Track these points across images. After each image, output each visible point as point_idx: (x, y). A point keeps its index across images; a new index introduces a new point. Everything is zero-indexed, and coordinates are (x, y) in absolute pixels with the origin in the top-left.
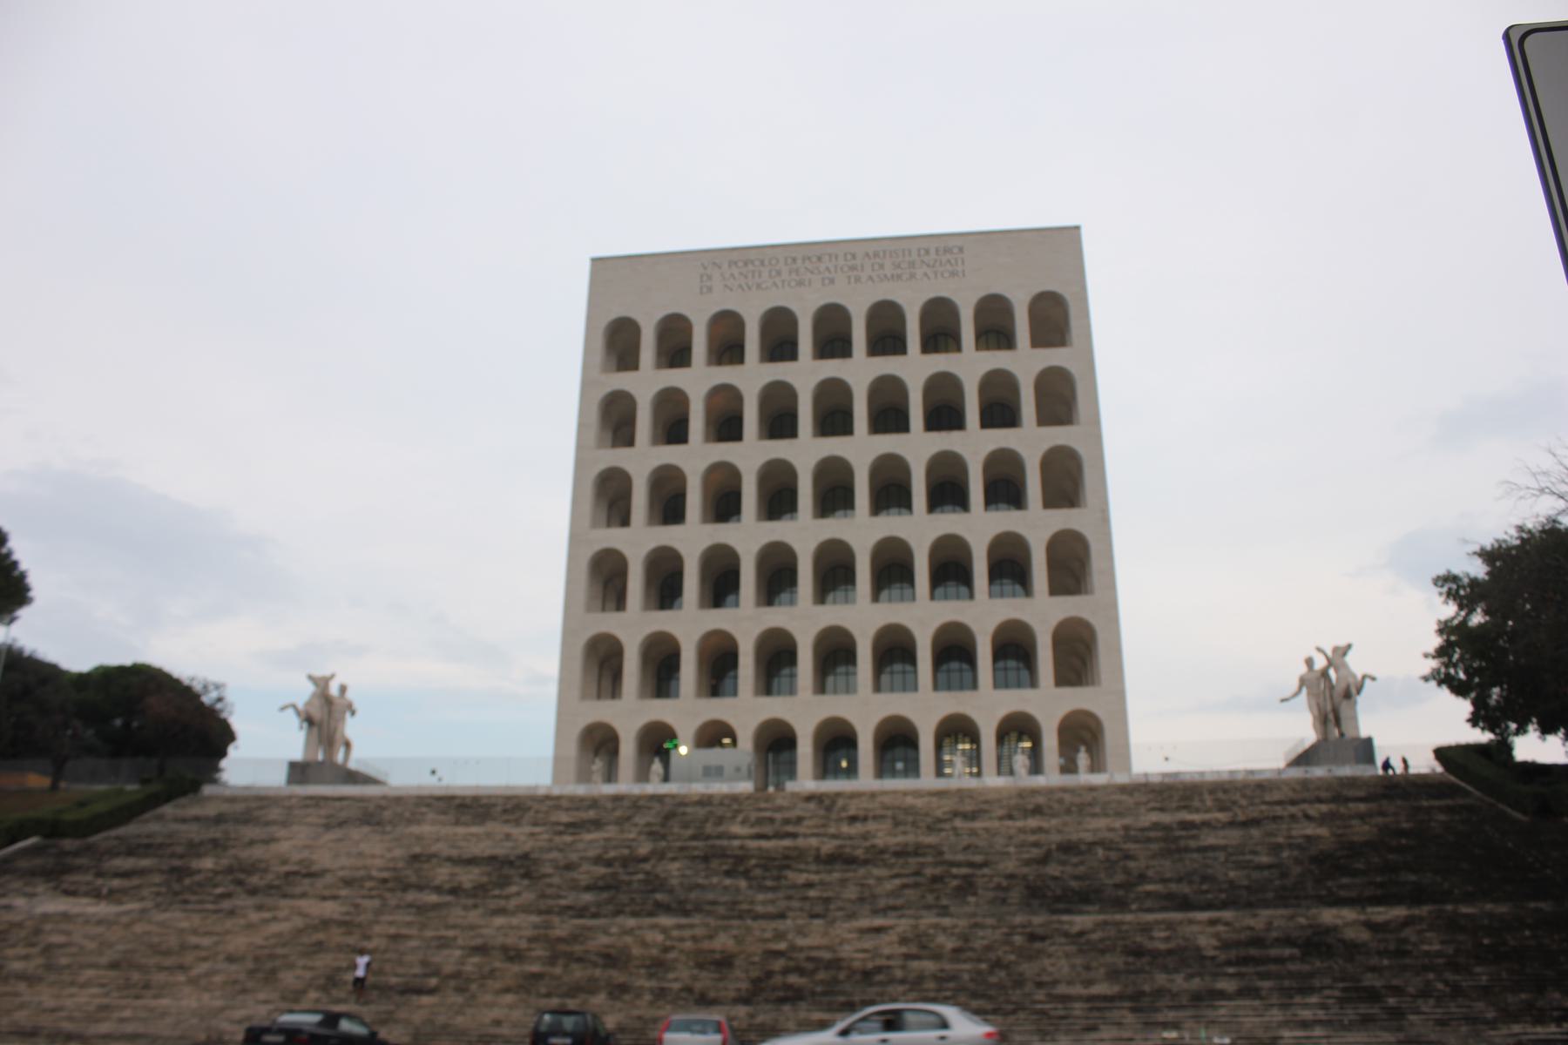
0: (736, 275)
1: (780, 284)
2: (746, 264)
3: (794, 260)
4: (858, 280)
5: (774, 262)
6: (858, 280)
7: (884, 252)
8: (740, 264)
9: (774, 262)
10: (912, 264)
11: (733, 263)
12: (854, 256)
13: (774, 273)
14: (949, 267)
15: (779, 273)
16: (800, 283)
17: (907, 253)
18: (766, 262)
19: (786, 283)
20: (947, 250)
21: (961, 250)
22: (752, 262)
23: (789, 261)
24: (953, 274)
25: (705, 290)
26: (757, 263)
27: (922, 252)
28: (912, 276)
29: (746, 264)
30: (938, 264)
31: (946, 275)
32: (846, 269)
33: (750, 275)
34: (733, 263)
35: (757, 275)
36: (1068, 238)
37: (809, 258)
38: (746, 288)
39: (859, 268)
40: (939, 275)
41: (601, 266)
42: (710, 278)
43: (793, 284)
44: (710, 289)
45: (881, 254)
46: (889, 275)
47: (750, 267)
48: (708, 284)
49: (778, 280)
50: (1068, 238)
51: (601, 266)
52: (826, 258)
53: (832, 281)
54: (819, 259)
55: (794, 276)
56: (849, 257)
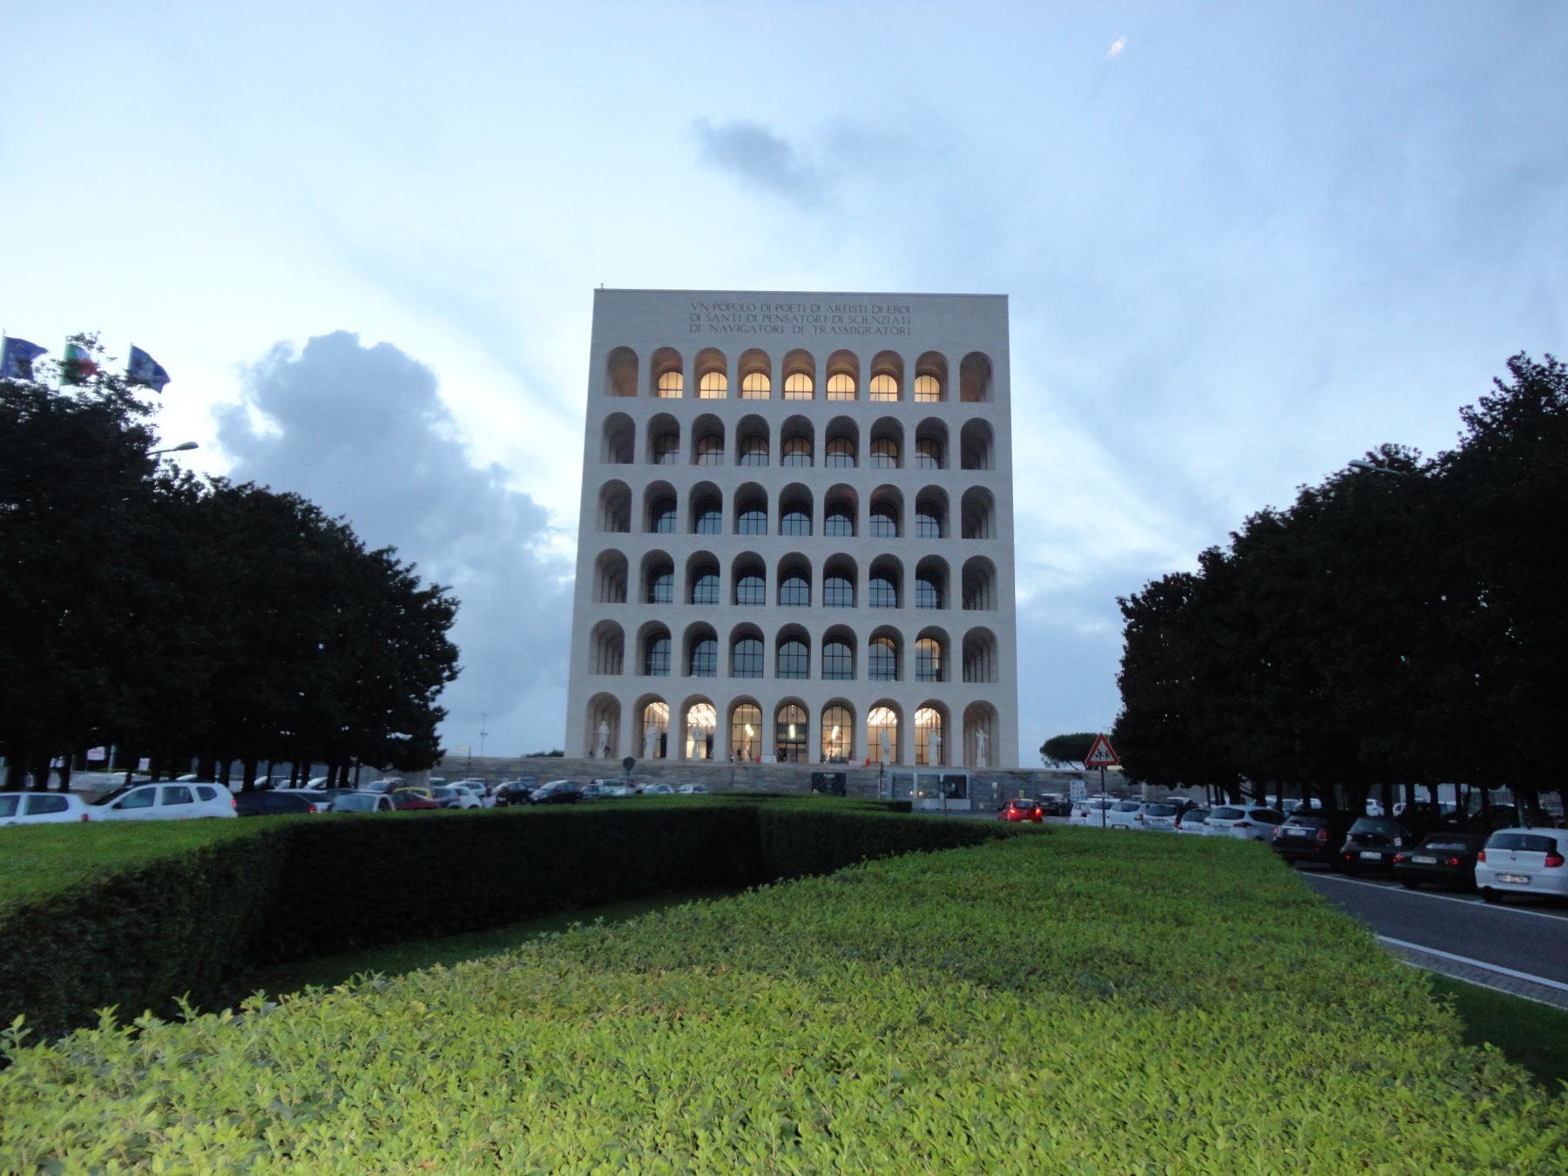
0: (720, 317)
1: (757, 329)
2: (728, 307)
3: (769, 308)
5: (752, 307)
6: (823, 330)
7: (844, 306)
8: (723, 307)
9: (752, 307)
10: (864, 320)
11: (717, 306)
12: (819, 308)
13: (751, 318)
14: (895, 324)
15: (755, 318)
16: (775, 329)
17: (863, 308)
18: (745, 309)
19: (763, 328)
20: (897, 309)
21: (908, 309)
22: (733, 306)
23: (765, 307)
24: (901, 331)
25: (694, 328)
26: (737, 307)
27: (876, 309)
29: (728, 307)
30: (886, 321)
31: (895, 331)
32: (811, 319)
33: (731, 318)
35: (737, 318)
36: (993, 309)
37: (781, 307)
38: (727, 328)
39: (823, 320)
40: (888, 332)
41: (609, 304)
42: (699, 317)
43: (768, 329)
44: (698, 328)
45: (842, 308)
46: (848, 329)
47: (731, 309)
48: (698, 323)
49: (754, 324)
50: (993, 309)
51: (605, 299)
52: (796, 308)
53: (801, 330)
54: (790, 308)
55: (767, 320)
56: (815, 308)
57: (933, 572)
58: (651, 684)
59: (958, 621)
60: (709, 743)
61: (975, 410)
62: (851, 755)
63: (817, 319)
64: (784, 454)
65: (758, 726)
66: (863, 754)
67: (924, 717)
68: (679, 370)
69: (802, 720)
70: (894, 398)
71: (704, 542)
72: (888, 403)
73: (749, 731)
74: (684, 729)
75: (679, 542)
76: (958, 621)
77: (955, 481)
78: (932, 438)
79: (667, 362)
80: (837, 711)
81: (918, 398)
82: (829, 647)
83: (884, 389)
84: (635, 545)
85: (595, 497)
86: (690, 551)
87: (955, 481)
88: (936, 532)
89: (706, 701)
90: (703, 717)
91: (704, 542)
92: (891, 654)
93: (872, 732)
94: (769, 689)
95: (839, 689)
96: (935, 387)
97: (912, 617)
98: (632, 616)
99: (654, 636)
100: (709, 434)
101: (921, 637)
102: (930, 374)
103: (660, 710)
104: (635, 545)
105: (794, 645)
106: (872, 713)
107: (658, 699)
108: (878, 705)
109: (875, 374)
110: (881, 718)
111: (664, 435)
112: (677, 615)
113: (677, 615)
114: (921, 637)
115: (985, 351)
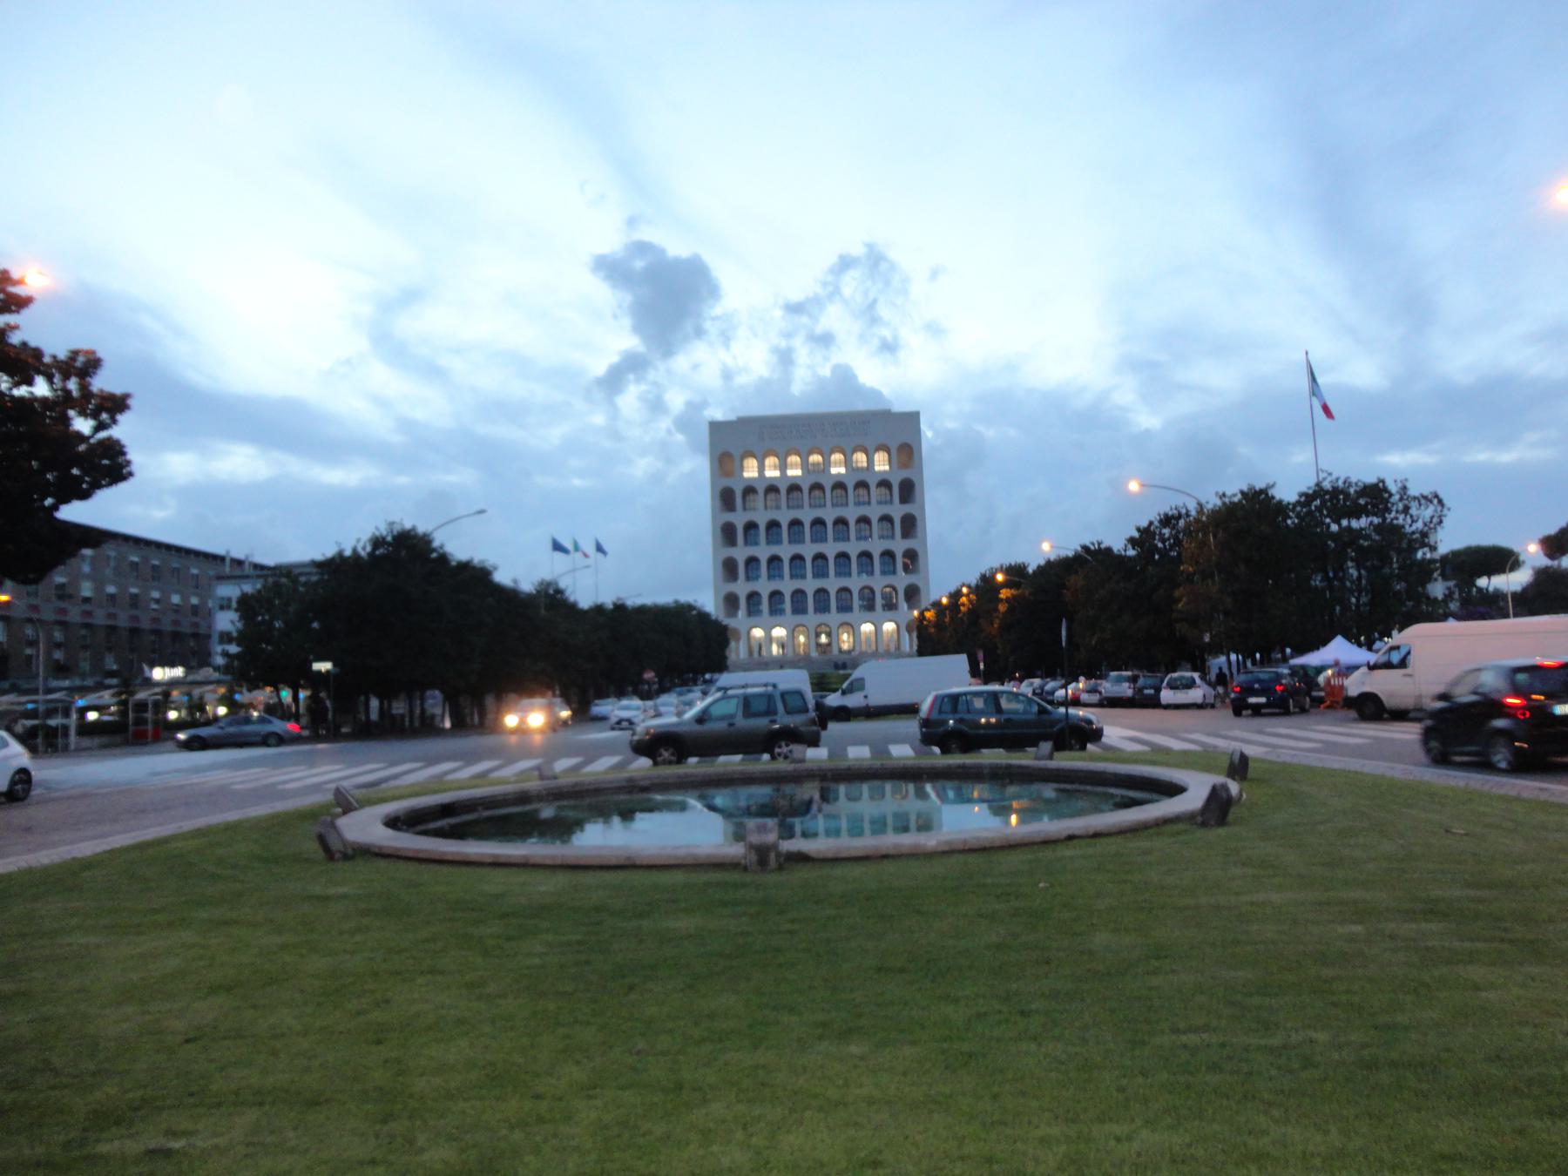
15: (791, 432)
21: (869, 422)
41: (717, 429)
50: (912, 419)
57: (888, 555)
58: (753, 620)
59: (902, 580)
60: (783, 646)
61: (905, 474)
62: (854, 647)
64: (810, 493)
65: (808, 637)
66: (857, 648)
67: (889, 627)
68: (753, 455)
69: (828, 630)
70: (865, 465)
71: (775, 550)
72: (862, 469)
73: (802, 639)
74: (769, 639)
75: (763, 552)
76: (902, 580)
77: (897, 511)
78: (885, 484)
79: (750, 454)
80: (846, 627)
81: (876, 463)
82: (839, 595)
83: (860, 459)
84: (740, 553)
85: (719, 530)
87: (897, 511)
88: (890, 534)
89: (780, 626)
90: (779, 632)
91: (775, 550)
92: (871, 596)
93: (863, 637)
94: (812, 618)
95: (846, 617)
96: (886, 455)
97: (878, 582)
98: (742, 588)
99: (753, 597)
100: (772, 489)
101: (888, 586)
102: (884, 450)
103: (758, 633)
104: (740, 553)
105: (822, 594)
106: (863, 625)
107: (756, 627)
108: (865, 623)
109: (855, 450)
110: (867, 628)
111: (749, 490)
112: (764, 586)
113: (764, 586)
114: (888, 586)
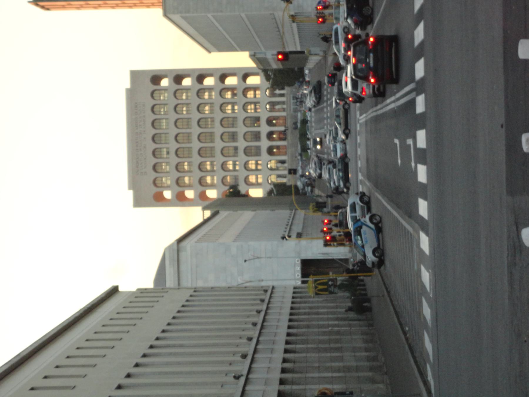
4: (144, 131)
6: (144, 131)
11: (137, 167)
12: (137, 133)
15: (141, 154)
16: (145, 147)
20: (136, 107)
21: (136, 103)
24: (144, 105)
28: (144, 116)
34: (137, 167)
36: (135, 75)
41: (138, 202)
44: (145, 172)
50: (135, 75)
53: (145, 138)
54: (137, 142)
63: (141, 133)
86: (222, 171)
115: (150, 77)
